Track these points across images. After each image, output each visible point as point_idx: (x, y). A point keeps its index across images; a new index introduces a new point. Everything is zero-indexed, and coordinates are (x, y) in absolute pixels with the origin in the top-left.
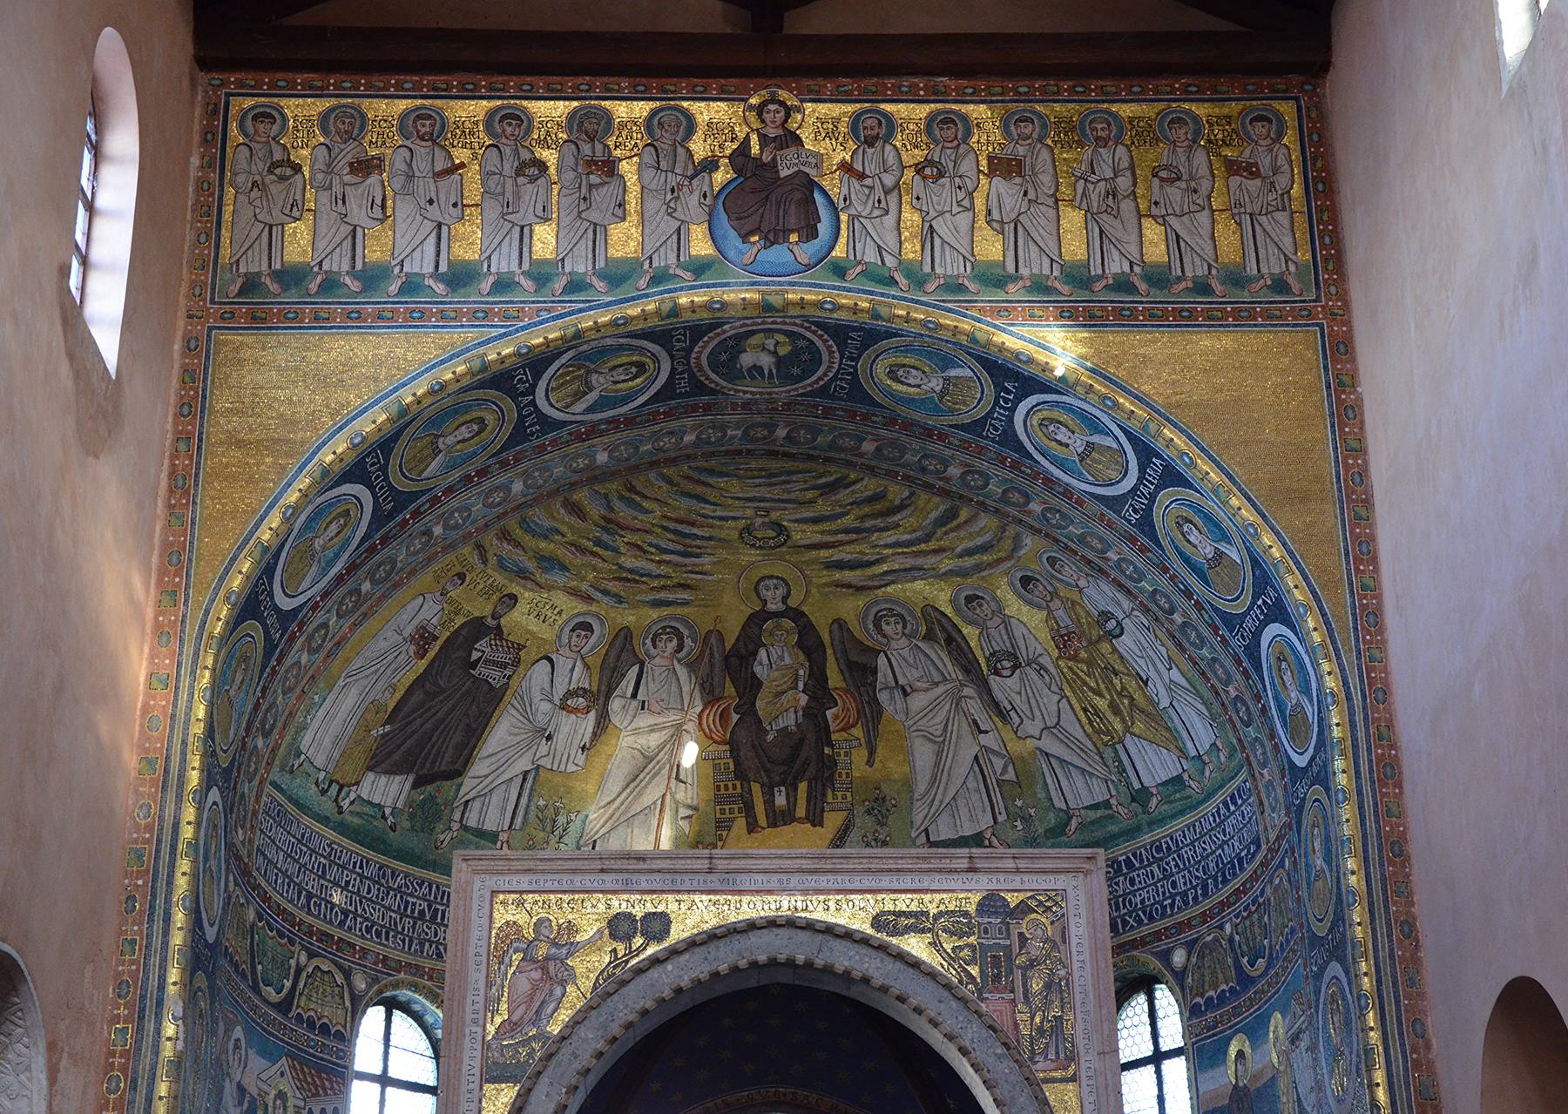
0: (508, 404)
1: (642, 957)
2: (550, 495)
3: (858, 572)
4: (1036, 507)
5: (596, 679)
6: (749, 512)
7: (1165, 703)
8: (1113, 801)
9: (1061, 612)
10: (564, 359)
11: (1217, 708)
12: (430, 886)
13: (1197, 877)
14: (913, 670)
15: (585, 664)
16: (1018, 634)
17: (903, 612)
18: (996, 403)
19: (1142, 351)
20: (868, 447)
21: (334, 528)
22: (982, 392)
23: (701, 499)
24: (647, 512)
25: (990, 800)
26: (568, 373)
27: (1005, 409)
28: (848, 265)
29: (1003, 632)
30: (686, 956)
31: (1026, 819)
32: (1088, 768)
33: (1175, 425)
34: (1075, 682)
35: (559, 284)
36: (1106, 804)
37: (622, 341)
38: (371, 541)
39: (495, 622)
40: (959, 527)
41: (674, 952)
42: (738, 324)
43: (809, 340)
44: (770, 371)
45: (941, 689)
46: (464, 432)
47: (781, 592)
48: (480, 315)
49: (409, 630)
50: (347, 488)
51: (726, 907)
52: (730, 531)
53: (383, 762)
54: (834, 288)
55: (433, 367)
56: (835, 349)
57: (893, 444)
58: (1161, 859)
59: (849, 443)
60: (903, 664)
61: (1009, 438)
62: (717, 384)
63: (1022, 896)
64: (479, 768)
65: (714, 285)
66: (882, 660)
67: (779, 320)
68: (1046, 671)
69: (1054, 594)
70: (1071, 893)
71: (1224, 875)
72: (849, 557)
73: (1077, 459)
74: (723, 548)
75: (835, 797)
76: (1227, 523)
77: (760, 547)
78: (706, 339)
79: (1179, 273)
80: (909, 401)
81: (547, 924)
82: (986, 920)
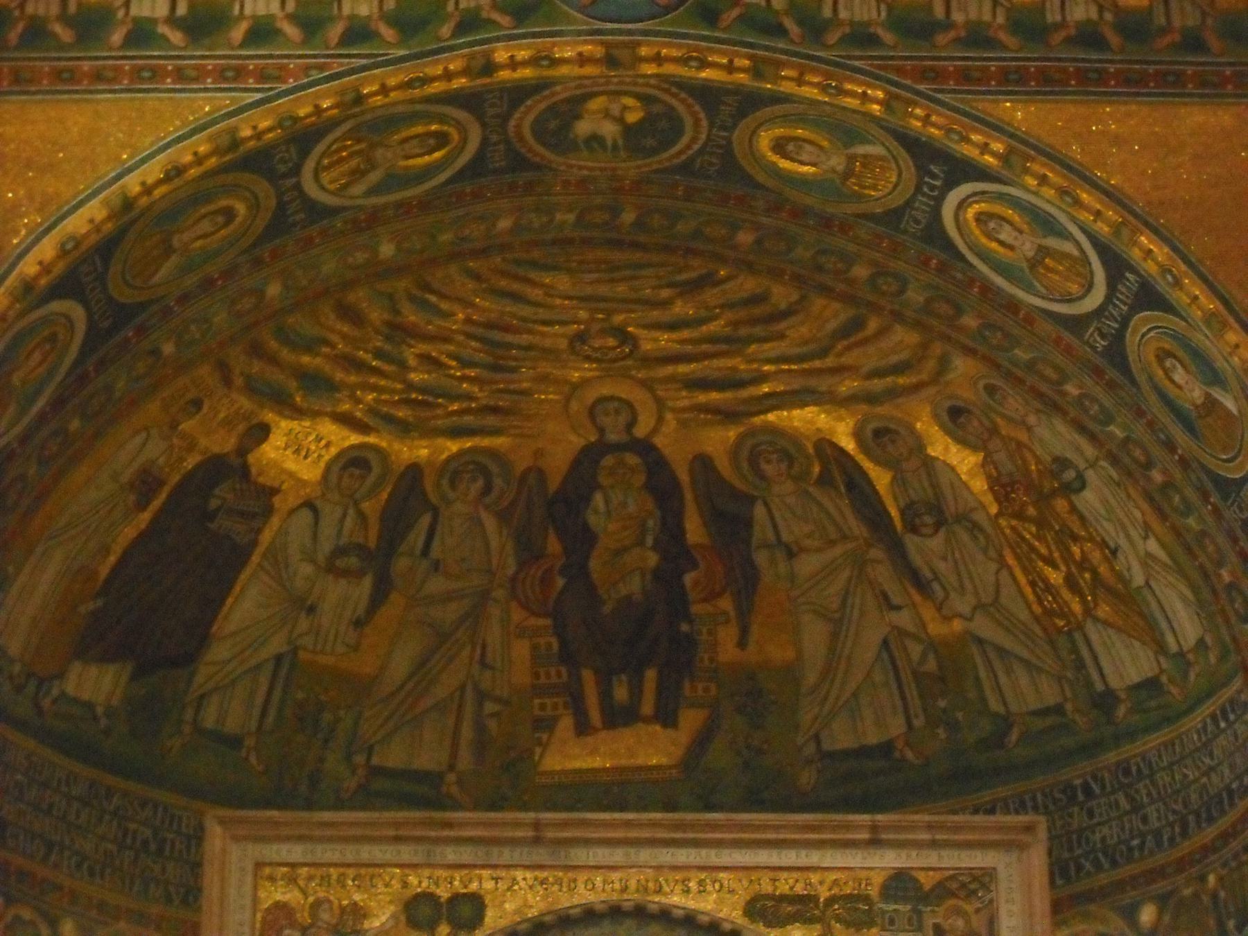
0: (263, 188)
3: (729, 395)
6: (583, 314)
7: (1138, 580)
8: (1069, 707)
10: (338, 132)
11: (1206, 594)
12: (156, 807)
13: (1174, 812)
15: (361, 515)
18: (918, 189)
20: (745, 238)
21: (37, 356)
22: (900, 175)
23: (515, 297)
24: (448, 315)
25: (903, 698)
26: (345, 148)
29: (924, 476)
31: (953, 726)
32: (1034, 660)
33: (1156, 231)
35: (335, 31)
36: (1058, 710)
37: (418, 107)
42: (573, 84)
44: (615, 141)
45: (838, 550)
46: (206, 226)
47: (622, 419)
48: (230, 74)
50: (56, 306)
51: (556, 887)
52: (557, 337)
54: (704, 38)
55: (168, 146)
56: (702, 115)
58: (1130, 785)
61: (934, 234)
62: (543, 157)
63: (938, 876)
64: (219, 652)
66: (759, 511)
67: (628, 80)
68: (981, 530)
69: (994, 431)
70: (1002, 874)
71: (1209, 810)
72: (717, 374)
73: (1025, 265)
76: (1220, 364)
77: (597, 360)
78: (529, 102)
79: (1163, 20)
80: (802, 183)
81: (326, 906)
82: (893, 907)
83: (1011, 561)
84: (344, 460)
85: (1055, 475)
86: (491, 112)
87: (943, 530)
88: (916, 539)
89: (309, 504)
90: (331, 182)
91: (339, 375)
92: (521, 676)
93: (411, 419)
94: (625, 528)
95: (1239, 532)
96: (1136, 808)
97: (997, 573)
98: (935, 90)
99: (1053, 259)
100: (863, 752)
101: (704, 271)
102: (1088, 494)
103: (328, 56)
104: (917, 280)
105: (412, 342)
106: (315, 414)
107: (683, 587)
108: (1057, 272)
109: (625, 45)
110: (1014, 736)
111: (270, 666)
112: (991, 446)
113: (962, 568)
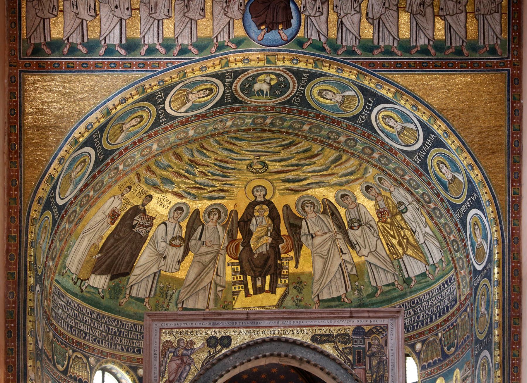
1: (220, 354)
2: (168, 150)
4: (376, 155)
5: (184, 231)
9: (381, 202)
16: (362, 211)
19: (430, 83)
22: (359, 103)
27: (368, 110)
28: (305, 41)
34: (384, 232)
35: (176, 50)
39: (143, 208)
42: (255, 70)
43: (285, 78)
45: (328, 235)
61: (368, 125)
65: (245, 51)
67: (273, 68)
68: (373, 227)
69: (379, 194)
75: (281, 281)
78: (240, 77)
83: (381, 237)
85: (398, 208)
87: (360, 227)
88: (352, 231)
92: (229, 278)
95: (459, 223)
96: (416, 313)
100: (333, 300)
103: (173, 59)
104: (361, 141)
106: (167, 192)
107: (279, 249)
108: (407, 136)
109: (273, 55)
110: (379, 292)
112: (378, 199)
113: (366, 240)
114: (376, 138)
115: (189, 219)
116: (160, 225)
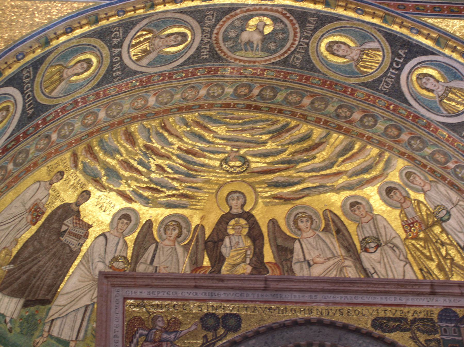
0: (106, 52)
4: (405, 137)
6: (229, 148)
9: (410, 209)
14: (316, 251)
16: (381, 225)
17: (311, 214)
18: (392, 64)
20: (306, 101)
22: (383, 59)
23: (201, 138)
24: (171, 144)
26: (142, 35)
27: (397, 69)
29: (372, 225)
30: (254, 341)
37: (177, 15)
38: (17, 134)
40: (353, 156)
41: (246, 338)
42: (245, 9)
44: (258, 45)
45: (331, 262)
46: (78, 69)
47: (241, 201)
49: (29, 205)
53: (8, 287)
56: (298, 30)
57: (323, 98)
59: (294, 98)
60: (309, 246)
64: (60, 300)
66: (297, 246)
68: (398, 247)
69: (407, 197)
72: (282, 179)
73: (437, 100)
74: (210, 172)
77: (231, 173)
78: (224, 19)
81: (160, 319)
82: (445, 325)
84: (120, 215)
86: (208, 23)
87: (379, 249)
88: (366, 254)
89: (104, 235)
90: (134, 55)
91: (122, 172)
93: (150, 197)
94: (238, 254)
97: (405, 266)
98: (404, 13)
99: (453, 93)
101: (285, 123)
102: (451, 221)
104: (383, 117)
105: (154, 157)
106: (111, 190)
111: (83, 310)
112: (404, 205)
113: (388, 266)
114: (406, 111)
115: (139, 234)
116: (98, 237)
